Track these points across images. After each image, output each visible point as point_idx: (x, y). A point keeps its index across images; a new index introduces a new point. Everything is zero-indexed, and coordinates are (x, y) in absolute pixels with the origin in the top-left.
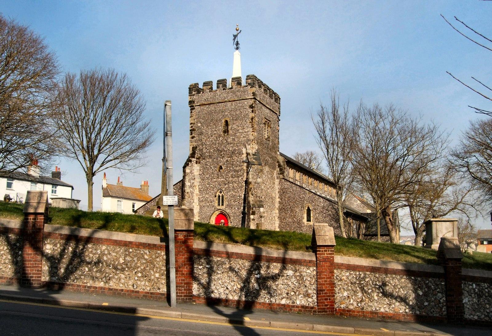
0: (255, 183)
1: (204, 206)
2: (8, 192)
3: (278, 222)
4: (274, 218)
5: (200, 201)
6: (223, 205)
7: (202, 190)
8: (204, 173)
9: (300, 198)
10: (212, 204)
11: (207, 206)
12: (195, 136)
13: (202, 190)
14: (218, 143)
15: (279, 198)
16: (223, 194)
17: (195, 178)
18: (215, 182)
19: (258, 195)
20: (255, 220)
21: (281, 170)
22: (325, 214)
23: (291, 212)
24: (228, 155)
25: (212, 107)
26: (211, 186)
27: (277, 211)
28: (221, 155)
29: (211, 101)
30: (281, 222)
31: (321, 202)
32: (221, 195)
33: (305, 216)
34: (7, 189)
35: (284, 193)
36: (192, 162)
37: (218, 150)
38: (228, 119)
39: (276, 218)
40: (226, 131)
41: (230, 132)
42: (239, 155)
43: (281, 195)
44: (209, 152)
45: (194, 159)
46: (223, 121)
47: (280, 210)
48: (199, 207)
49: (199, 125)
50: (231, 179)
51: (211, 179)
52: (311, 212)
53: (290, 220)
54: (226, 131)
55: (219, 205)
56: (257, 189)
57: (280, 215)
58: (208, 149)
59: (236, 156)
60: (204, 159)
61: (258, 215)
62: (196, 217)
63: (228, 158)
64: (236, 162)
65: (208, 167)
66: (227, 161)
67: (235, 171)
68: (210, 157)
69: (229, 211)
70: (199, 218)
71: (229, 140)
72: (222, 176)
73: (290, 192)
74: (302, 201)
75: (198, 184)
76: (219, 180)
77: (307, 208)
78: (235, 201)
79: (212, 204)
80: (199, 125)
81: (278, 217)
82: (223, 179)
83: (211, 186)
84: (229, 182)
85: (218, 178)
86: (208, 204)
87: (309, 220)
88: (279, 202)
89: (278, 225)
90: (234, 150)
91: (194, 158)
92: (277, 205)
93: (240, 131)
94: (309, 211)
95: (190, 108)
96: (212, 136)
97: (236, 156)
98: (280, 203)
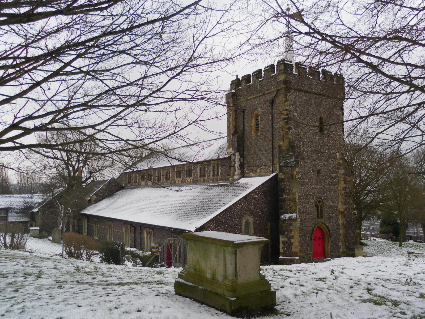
1: (305, 219)
6: (322, 217)
7: (302, 198)
8: (304, 177)
10: (312, 216)
11: (308, 218)
12: (292, 127)
13: (302, 198)
16: (323, 205)
18: (314, 188)
24: (325, 158)
26: (311, 193)
28: (319, 157)
42: (334, 159)
46: (319, 117)
49: (295, 114)
50: (328, 186)
51: (311, 185)
55: (318, 217)
58: (305, 148)
59: (332, 161)
60: (302, 159)
65: (307, 169)
66: (324, 164)
67: (332, 178)
68: (309, 158)
70: (299, 234)
72: (320, 182)
76: (318, 186)
78: (332, 213)
79: (312, 216)
80: (295, 114)
83: (311, 193)
84: (326, 190)
86: (308, 216)
90: (330, 153)
96: (309, 132)
97: (332, 161)
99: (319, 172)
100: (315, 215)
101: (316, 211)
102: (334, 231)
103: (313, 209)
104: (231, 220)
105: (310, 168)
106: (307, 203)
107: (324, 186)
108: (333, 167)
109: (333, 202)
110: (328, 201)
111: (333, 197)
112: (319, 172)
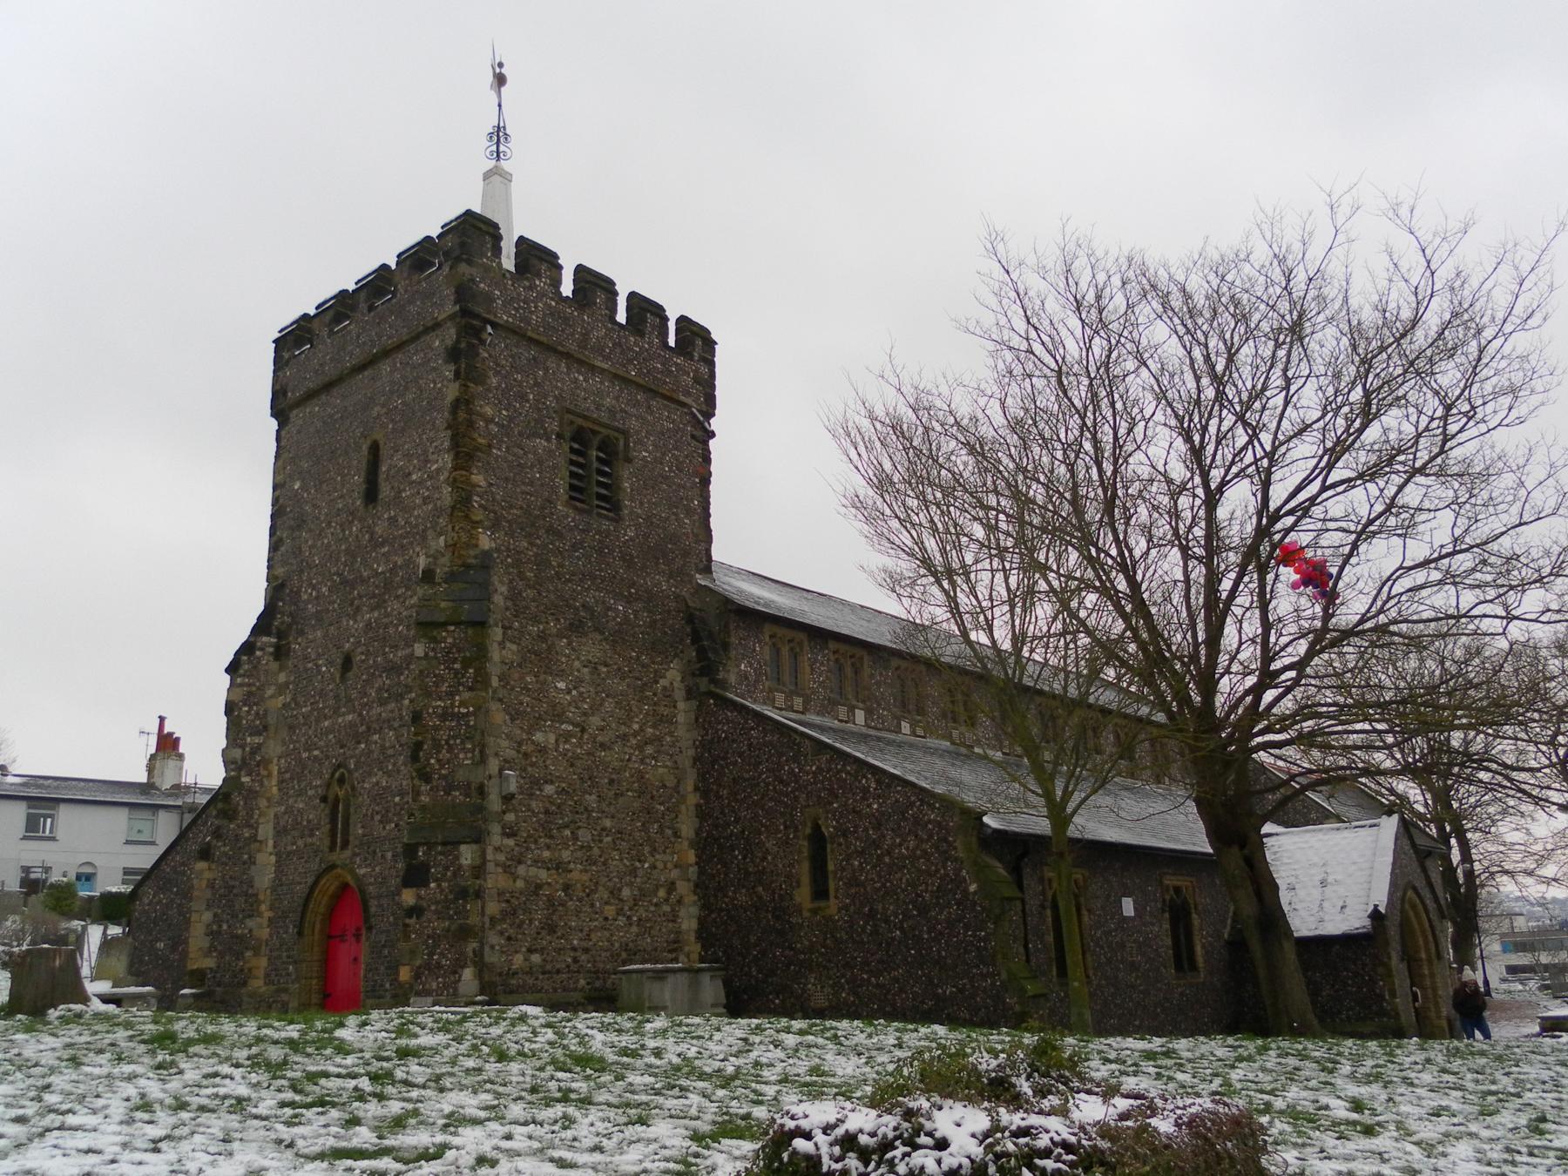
0: (444, 716)
1: (289, 854)
2: (35, 854)
3: (694, 910)
4: (662, 893)
5: (280, 832)
9: (781, 781)
14: (347, 552)
15: (696, 789)
17: (266, 728)
18: (329, 731)
19: (461, 775)
20: (428, 915)
21: (702, 653)
22: (889, 853)
23: (744, 858)
25: (335, 400)
26: (316, 753)
27: (691, 857)
29: (331, 371)
30: (706, 906)
31: (865, 790)
32: (341, 794)
33: (804, 871)
34: (25, 838)
35: (714, 762)
36: (258, 653)
37: (345, 582)
38: (378, 436)
39: (683, 888)
40: (371, 495)
41: (385, 491)
42: (408, 588)
43: (702, 776)
44: (317, 598)
45: (265, 639)
47: (702, 844)
48: (273, 858)
51: (318, 721)
52: (829, 846)
53: (742, 898)
54: (371, 495)
56: (450, 749)
57: (701, 872)
61: (444, 885)
62: (263, 907)
63: (372, 610)
64: (397, 626)
66: (368, 624)
69: (362, 871)
71: (379, 530)
72: (350, 700)
73: (741, 755)
74: (787, 795)
75: (279, 750)
77: (808, 831)
81: (697, 886)
82: (350, 717)
84: (369, 729)
85: (336, 712)
86: (300, 843)
87: (820, 893)
88: (698, 806)
89: (694, 924)
91: (269, 634)
92: (687, 827)
93: (414, 477)
94: (818, 841)
95: (274, 424)
97: (397, 597)
98: (702, 814)
99: (347, 663)
100: (321, 837)
101: (325, 821)
102: (384, 902)
103: (316, 814)
104: (184, 873)
105: (319, 656)
106: (301, 793)
107: (360, 715)
108: (401, 621)
109: (388, 774)
110: (370, 774)
111: (390, 752)
112: (347, 663)
